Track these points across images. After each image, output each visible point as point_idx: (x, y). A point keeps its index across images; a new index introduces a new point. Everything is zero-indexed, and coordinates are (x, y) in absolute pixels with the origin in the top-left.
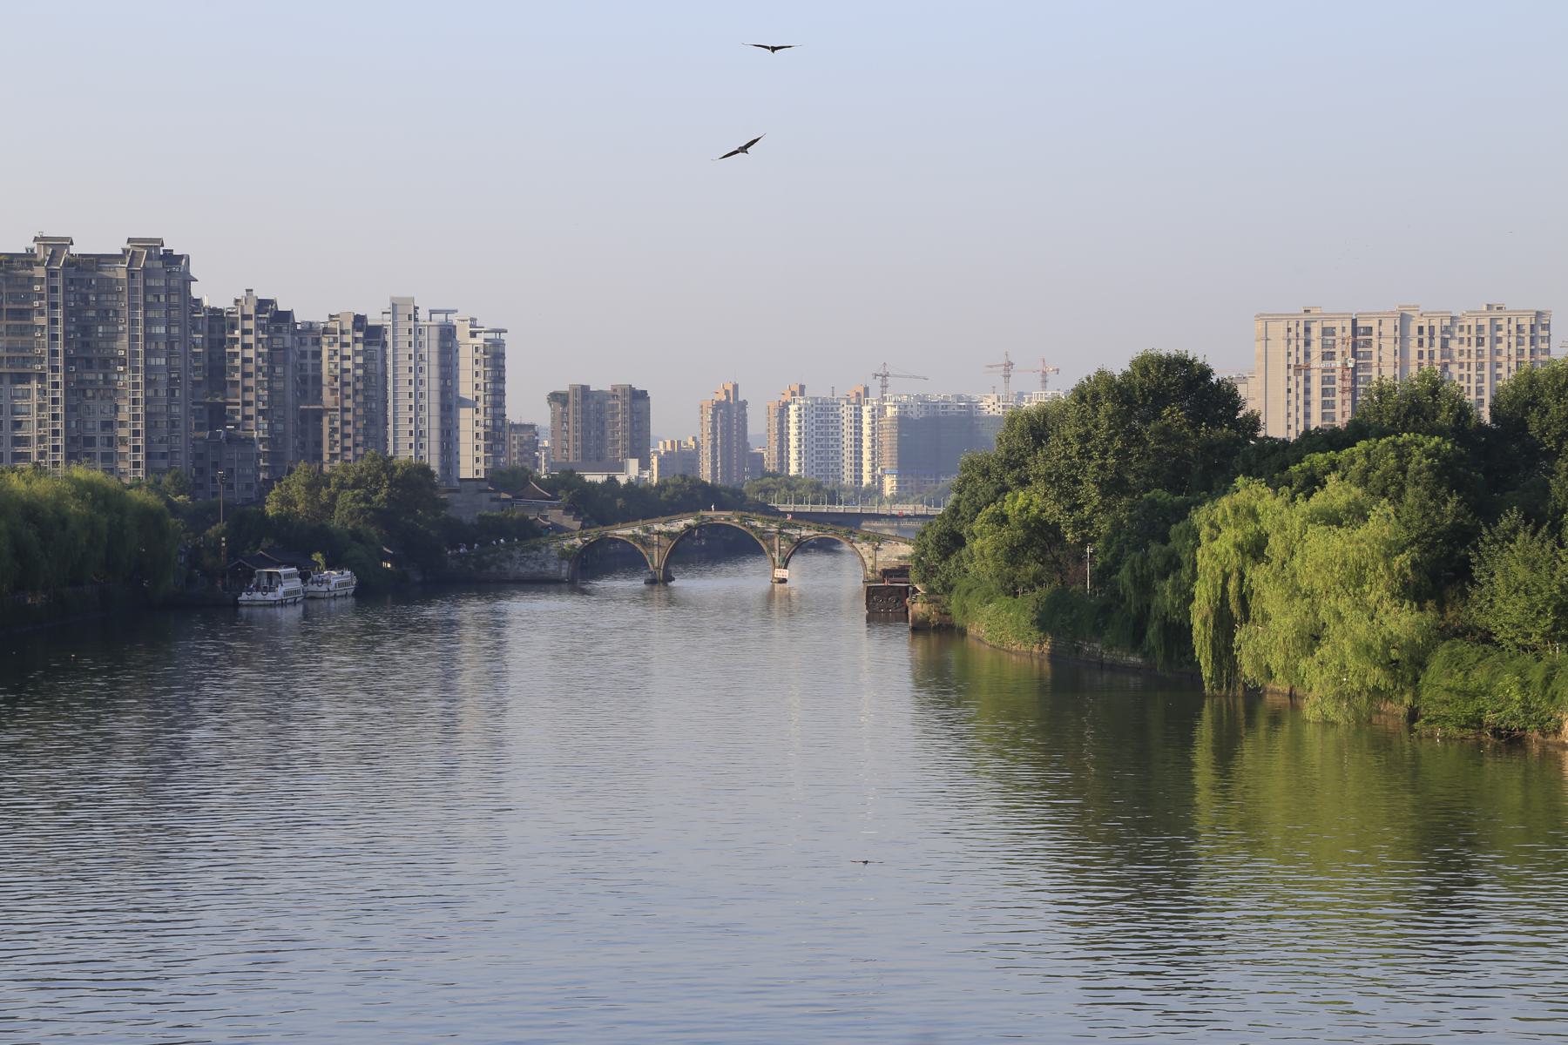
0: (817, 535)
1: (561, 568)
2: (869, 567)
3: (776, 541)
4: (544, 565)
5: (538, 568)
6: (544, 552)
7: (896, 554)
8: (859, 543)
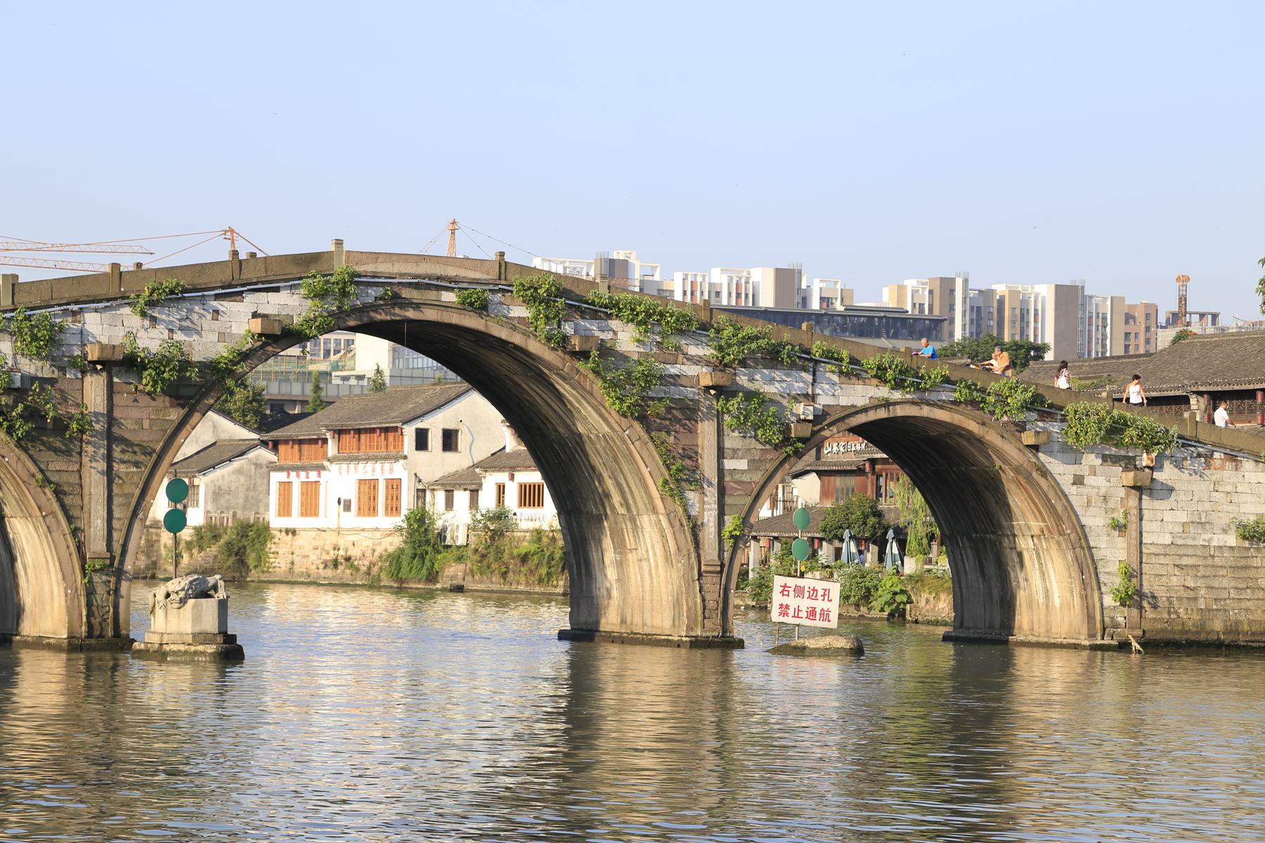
0: (887, 404)
2: (1112, 578)
3: (706, 431)
8: (1071, 453)
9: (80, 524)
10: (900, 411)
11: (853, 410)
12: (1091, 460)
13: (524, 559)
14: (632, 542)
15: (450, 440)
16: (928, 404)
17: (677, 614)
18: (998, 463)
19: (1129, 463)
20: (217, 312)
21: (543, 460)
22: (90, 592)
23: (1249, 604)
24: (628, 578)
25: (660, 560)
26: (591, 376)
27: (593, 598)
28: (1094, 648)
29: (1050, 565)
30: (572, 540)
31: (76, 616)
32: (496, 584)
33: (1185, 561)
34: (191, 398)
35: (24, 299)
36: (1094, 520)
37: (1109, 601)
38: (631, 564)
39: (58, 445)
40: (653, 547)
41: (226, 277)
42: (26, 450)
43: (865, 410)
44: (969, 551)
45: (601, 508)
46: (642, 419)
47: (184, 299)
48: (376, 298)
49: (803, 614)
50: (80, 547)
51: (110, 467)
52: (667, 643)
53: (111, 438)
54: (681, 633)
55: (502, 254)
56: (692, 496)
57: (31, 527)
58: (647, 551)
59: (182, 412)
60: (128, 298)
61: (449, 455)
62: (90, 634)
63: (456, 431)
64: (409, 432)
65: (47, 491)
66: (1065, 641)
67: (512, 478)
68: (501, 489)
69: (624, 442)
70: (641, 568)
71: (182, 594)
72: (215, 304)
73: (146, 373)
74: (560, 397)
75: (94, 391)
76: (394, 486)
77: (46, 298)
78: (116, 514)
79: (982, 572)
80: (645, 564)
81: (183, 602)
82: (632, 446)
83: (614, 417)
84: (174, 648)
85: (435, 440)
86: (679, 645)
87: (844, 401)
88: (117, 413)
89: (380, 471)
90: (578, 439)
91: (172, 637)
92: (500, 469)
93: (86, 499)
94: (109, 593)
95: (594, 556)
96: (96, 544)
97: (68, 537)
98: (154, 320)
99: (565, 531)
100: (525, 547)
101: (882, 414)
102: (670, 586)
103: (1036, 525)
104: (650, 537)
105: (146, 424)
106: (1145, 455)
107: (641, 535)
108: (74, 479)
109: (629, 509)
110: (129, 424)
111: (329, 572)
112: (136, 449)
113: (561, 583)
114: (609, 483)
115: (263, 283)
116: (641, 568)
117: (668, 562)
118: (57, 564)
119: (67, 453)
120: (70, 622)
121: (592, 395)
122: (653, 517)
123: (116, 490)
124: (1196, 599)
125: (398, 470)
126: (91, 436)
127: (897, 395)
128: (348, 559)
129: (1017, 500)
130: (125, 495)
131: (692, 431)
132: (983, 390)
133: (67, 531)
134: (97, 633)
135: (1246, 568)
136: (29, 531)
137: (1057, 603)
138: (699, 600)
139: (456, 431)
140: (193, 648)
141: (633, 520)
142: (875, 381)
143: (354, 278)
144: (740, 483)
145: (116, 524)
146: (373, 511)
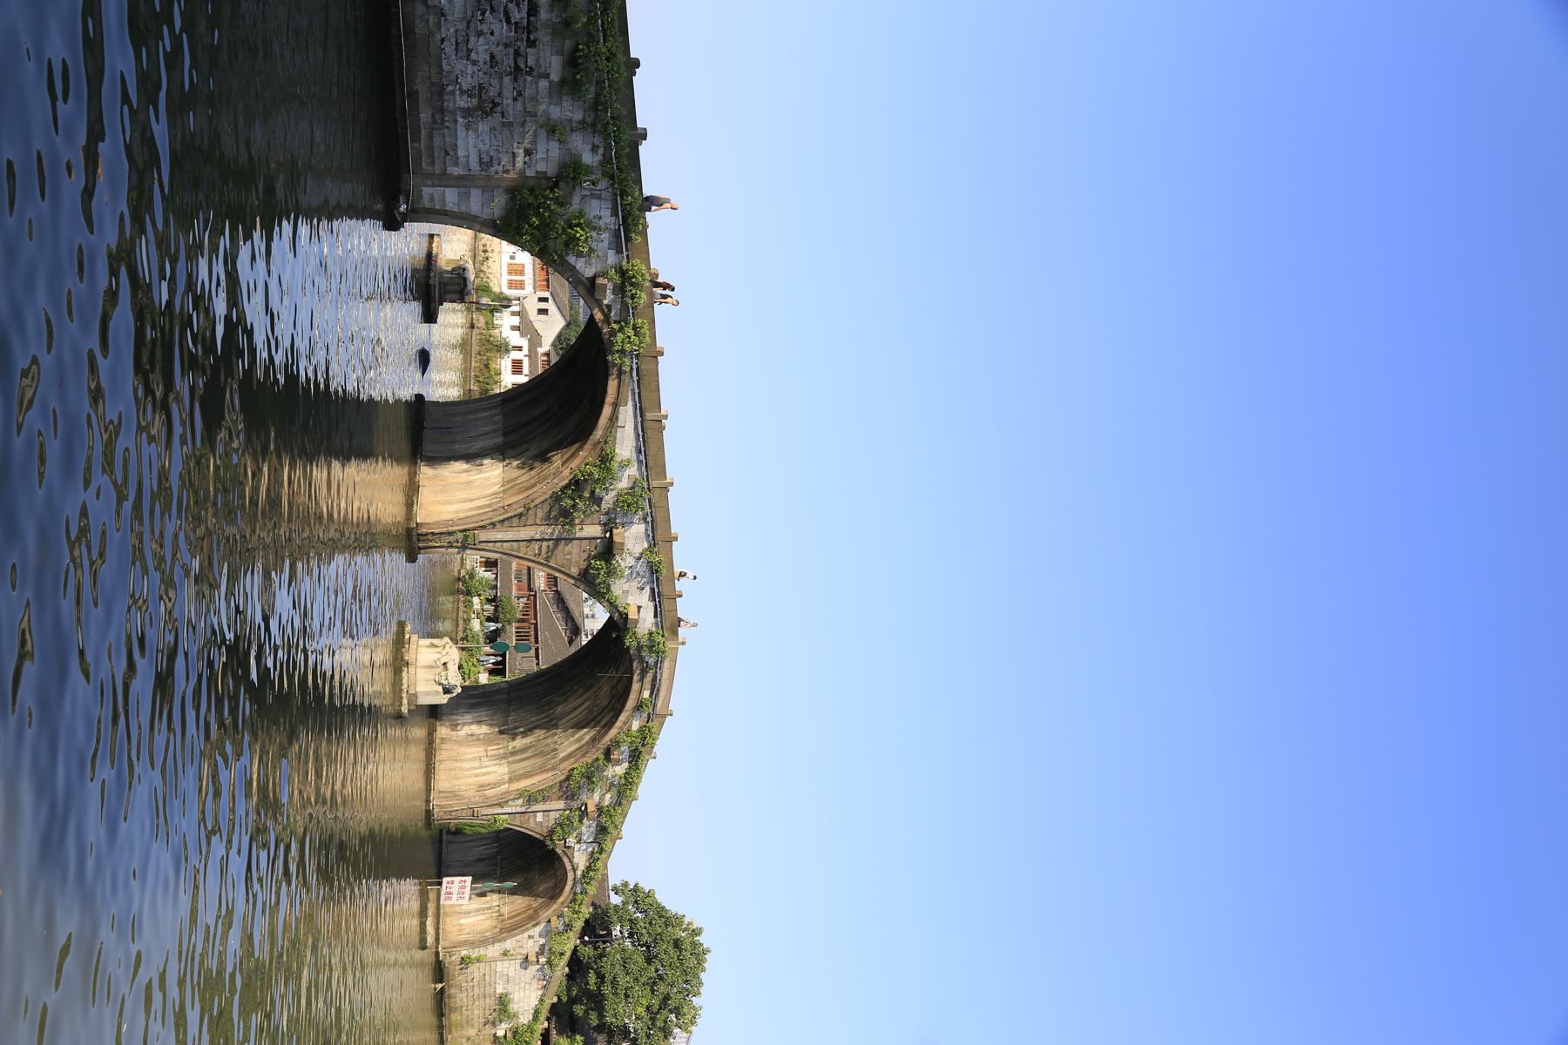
0: (574, 870)
1: (464, 182)
2: (474, 954)
3: (561, 804)
4: (486, 107)
5: (467, 82)
6: (556, 112)
7: (510, 988)
9: (498, 526)
10: (570, 875)
11: (571, 857)
12: (542, 941)
13: (487, 366)
14: (493, 753)
15: (543, 312)
16: (574, 884)
17: (445, 795)
18: (540, 900)
19: (538, 955)
20: (643, 589)
21: (542, 679)
22: (450, 534)
23: (465, 1000)
24: (470, 746)
25: (480, 779)
26: (595, 757)
27: (457, 709)
28: (437, 954)
29: (483, 917)
30: (494, 691)
31: (433, 526)
32: (475, 348)
33: (487, 977)
34: (585, 579)
35: (655, 496)
36: (509, 944)
37: (464, 953)
38: (478, 749)
39: (553, 514)
40: (488, 773)
41: (665, 590)
42: (551, 497)
43: (571, 861)
44: (490, 851)
45: (512, 726)
46: (568, 778)
47: (652, 573)
48: (647, 662)
49: (448, 890)
50: (483, 527)
51: (538, 540)
52: (428, 790)
53: (558, 540)
54: (435, 801)
55: (671, 715)
56: (521, 801)
57: (496, 488)
58: (486, 767)
59: (576, 575)
60: (654, 546)
61: (536, 311)
62: (418, 535)
63: (547, 314)
64: (547, 294)
65: (522, 509)
66: (441, 931)
67: (525, 356)
68: (520, 348)
69: (554, 768)
70: (474, 759)
71: (445, 683)
72: (648, 589)
73: (603, 563)
74: (579, 726)
75: (594, 530)
76: (521, 285)
77: (657, 505)
78: (505, 544)
79: (479, 860)
80: (476, 764)
81: (440, 684)
82: (550, 774)
83: (567, 765)
84: (405, 681)
85: (543, 305)
86: (428, 801)
87: (576, 854)
88: (575, 542)
89: (528, 278)
90: (550, 725)
91: (413, 677)
92: (529, 350)
93: (514, 529)
94: (449, 542)
95: (482, 713)
96: (483, 535)
97: (489, 521)
98: (639, 559)
99: (498, 685)
100: (493, 366)
101: (569, 867)
102: (464, 788)
103: (506, 910)
104: (495, 772)
105: (567, 557)
106: (544, 960)
107: (496, 762)
108: (530, 522)
109: (513, 754)
110: (568, 548)
111: (481, 248)
112: (550, 553)
113: (475, 388)
114: (528, 740)
115: (661, 611)
116: (474, 759)
117: (481, 786)
118: (470, 514)
119: (548, 517)
120: (428, 523)
121: (584, 756)
122: (507, 777)
123: (522, 543)
124: (467, 982)
125: (529, 288)
126: (559, 531)
127: (579, 873)
128: (487, 259)
129: (519, 902)
130: (519, 548)
131: (559, 799)
132: (581, 904)
133: (493, 520)
134: (421, 538)
135: (485, 997)
136: (494, 484)
137: (462, 921)
138: (456, 809)
139: (547, 314)
140: (404, 695)
141: (504, 757)
142: (588, 864)
143: (660, 655)
144: (529, 819)
145: (499, 544)
146: (510, 273)
